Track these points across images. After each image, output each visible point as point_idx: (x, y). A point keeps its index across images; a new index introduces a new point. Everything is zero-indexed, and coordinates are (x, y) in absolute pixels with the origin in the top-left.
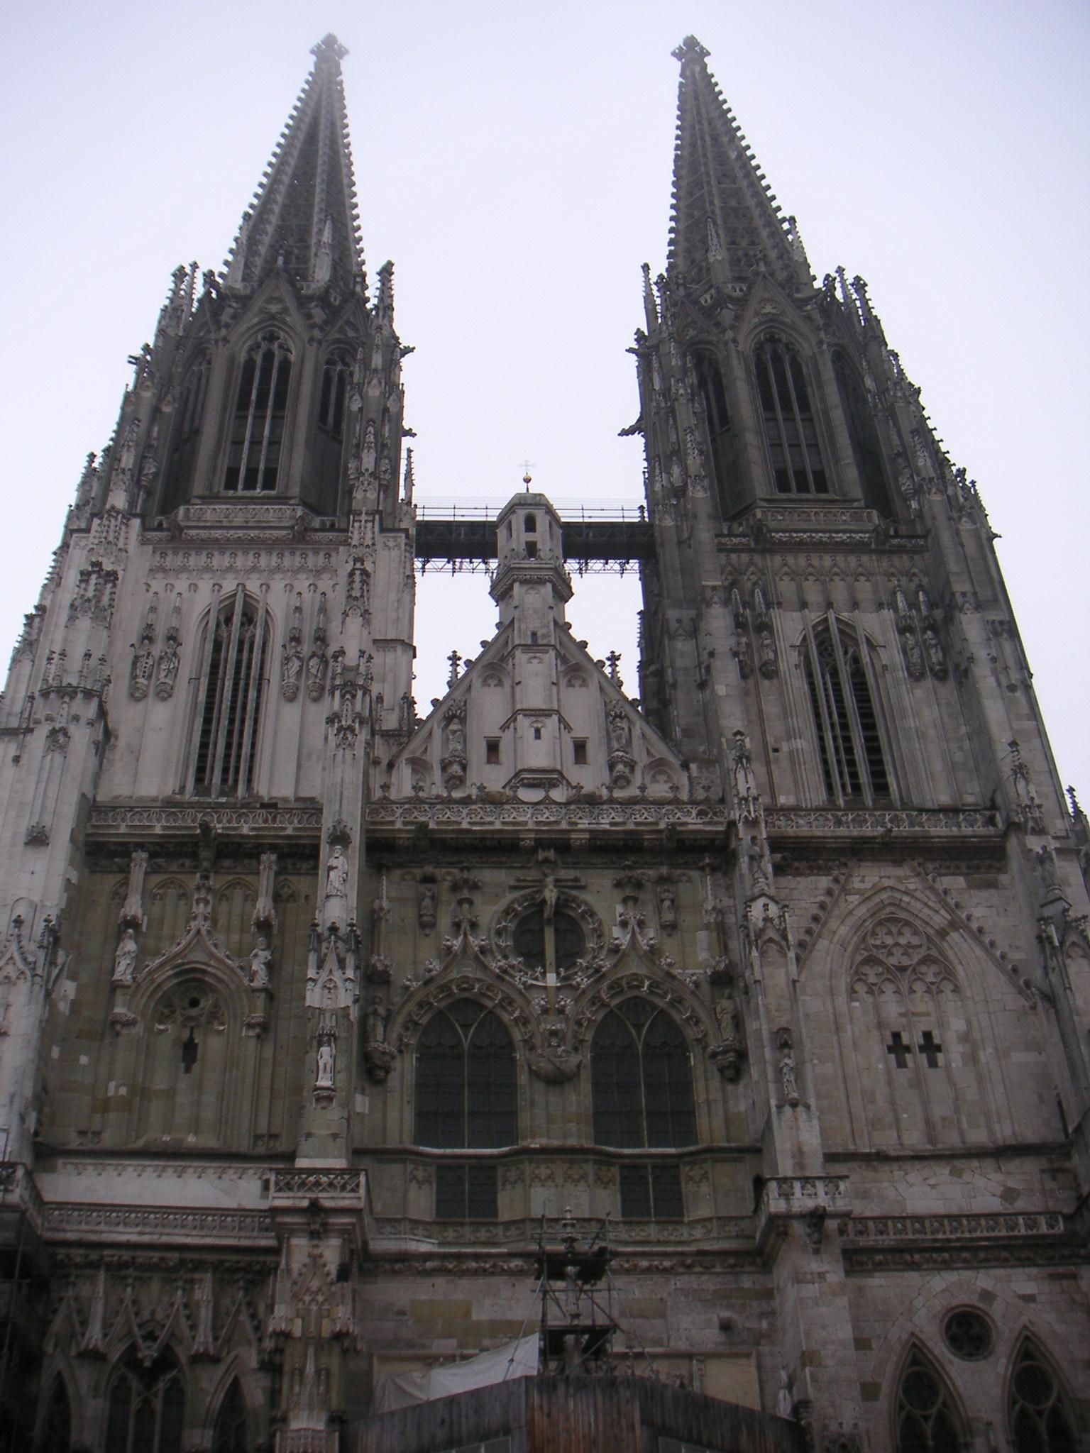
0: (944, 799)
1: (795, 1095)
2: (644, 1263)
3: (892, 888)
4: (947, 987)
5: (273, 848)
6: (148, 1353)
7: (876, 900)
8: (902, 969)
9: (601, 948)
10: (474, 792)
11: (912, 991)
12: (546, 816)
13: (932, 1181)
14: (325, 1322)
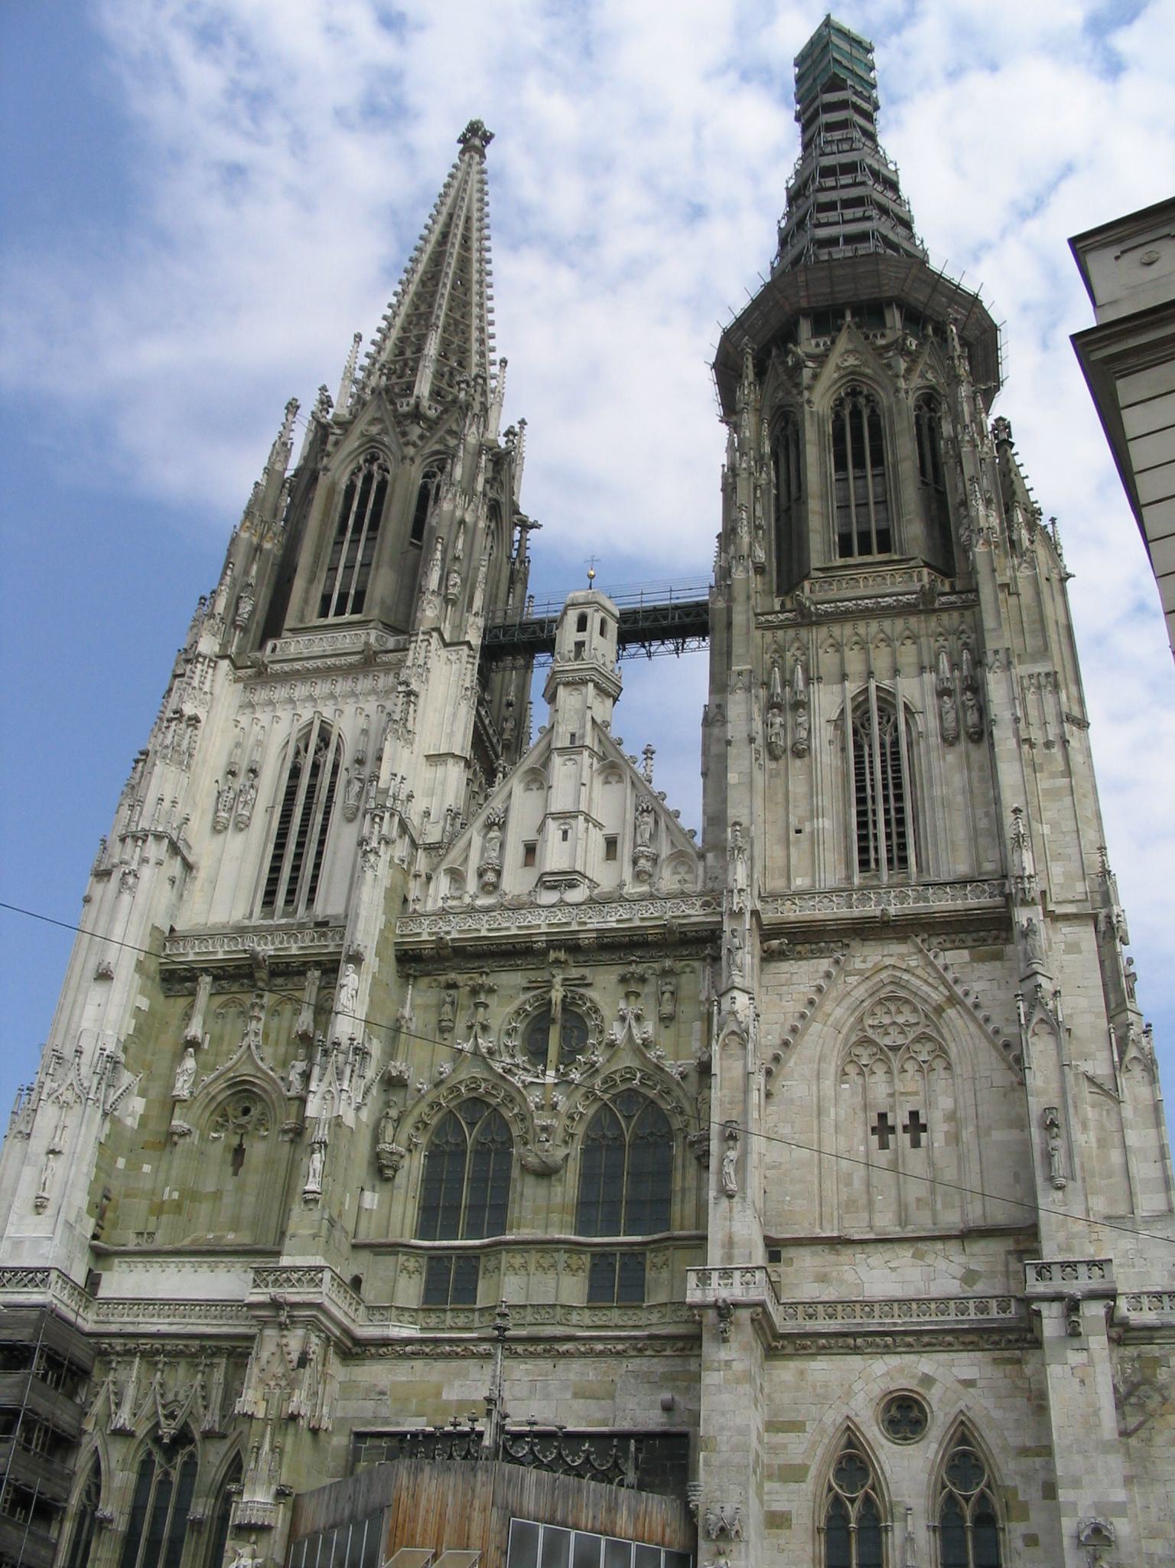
2: (600, 1347)
4: (939, 1064)
6: (168, 1430)
8: (895, 1049)
9: (600, 1043)
12: (560, 917)
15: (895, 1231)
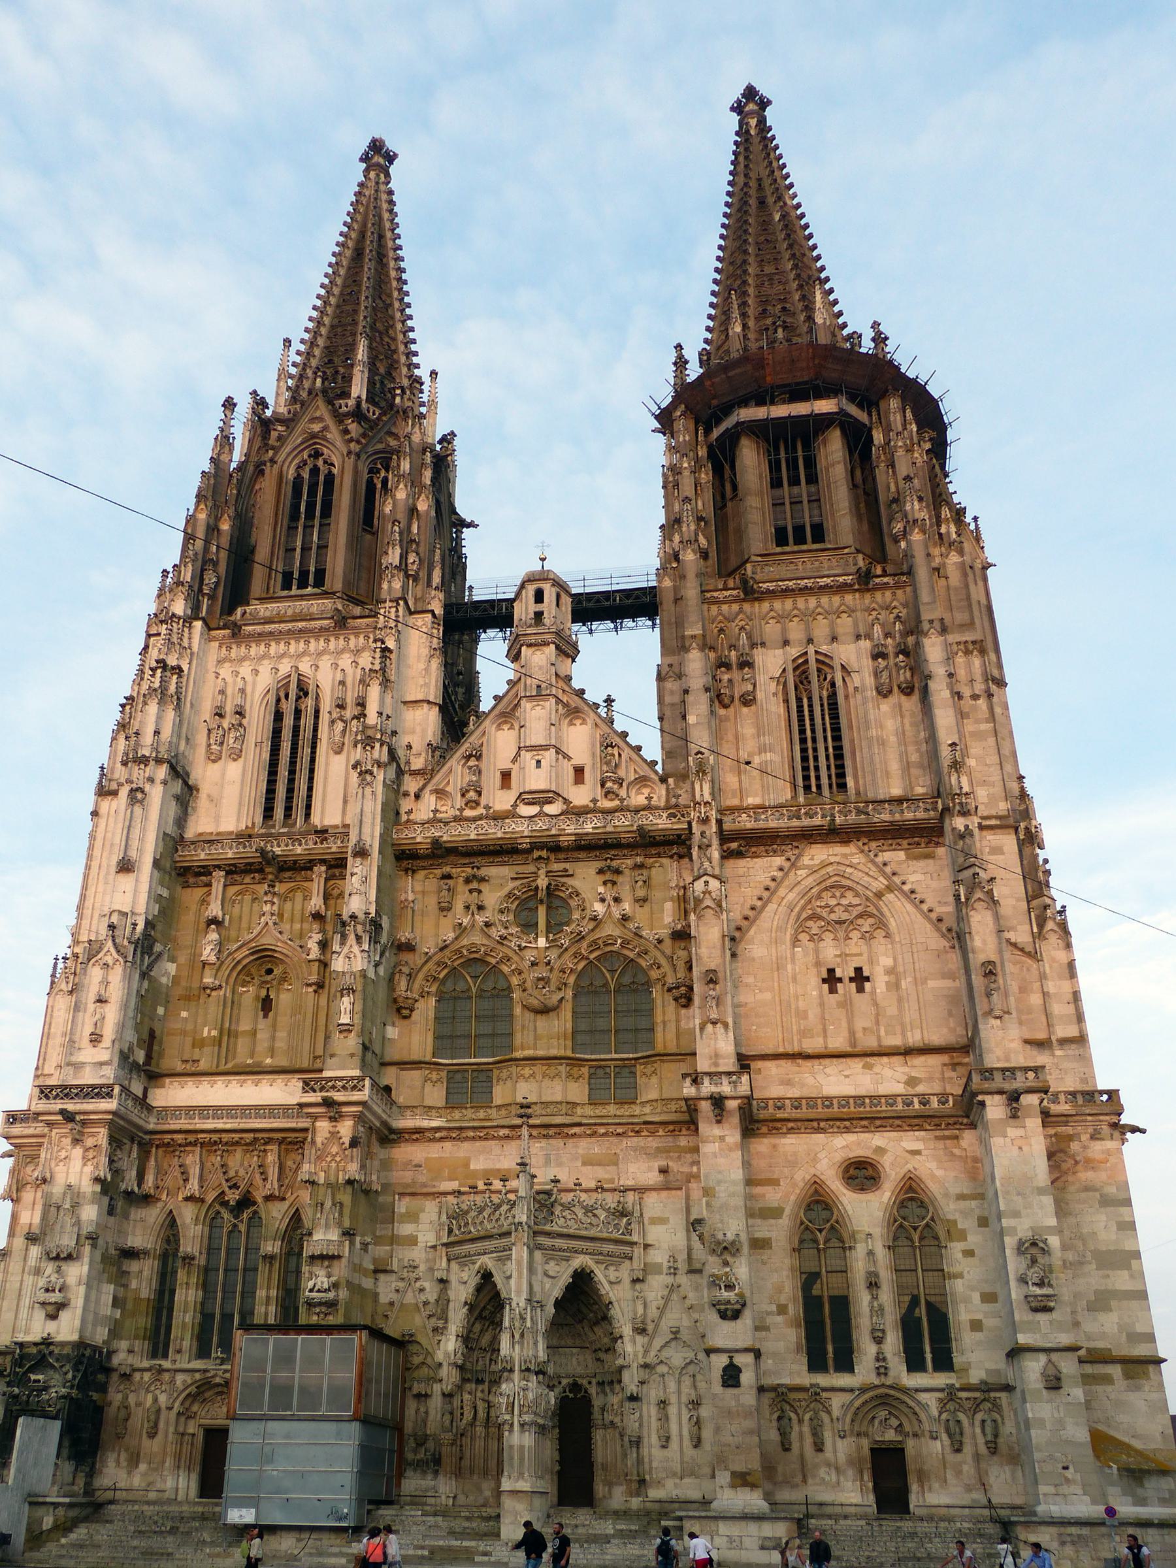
2: (602, 1130)
8: (840, 922)
13: (846, 1073)
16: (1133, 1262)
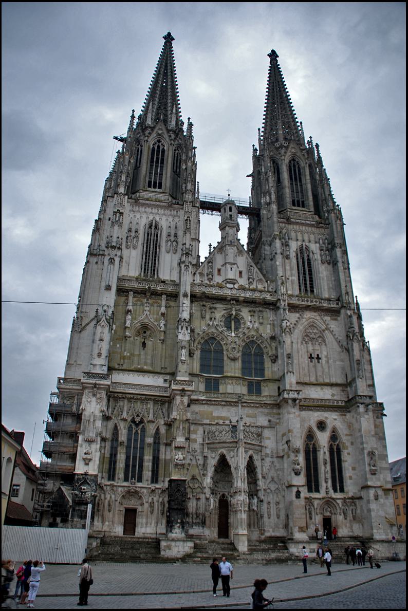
0: (327, 296)
1: (291, 370)
2: (252, 405)
3: (313, 318)
4: (323, 344)
5: (165, 294)
6: (137, 420)
7: (309, 321)
8: (314, 338)
10: (215, 283)
11: (315, 344)
12: (234, 292)
14: (184, 416)
15: (315, 382)
16: (386, 458)
